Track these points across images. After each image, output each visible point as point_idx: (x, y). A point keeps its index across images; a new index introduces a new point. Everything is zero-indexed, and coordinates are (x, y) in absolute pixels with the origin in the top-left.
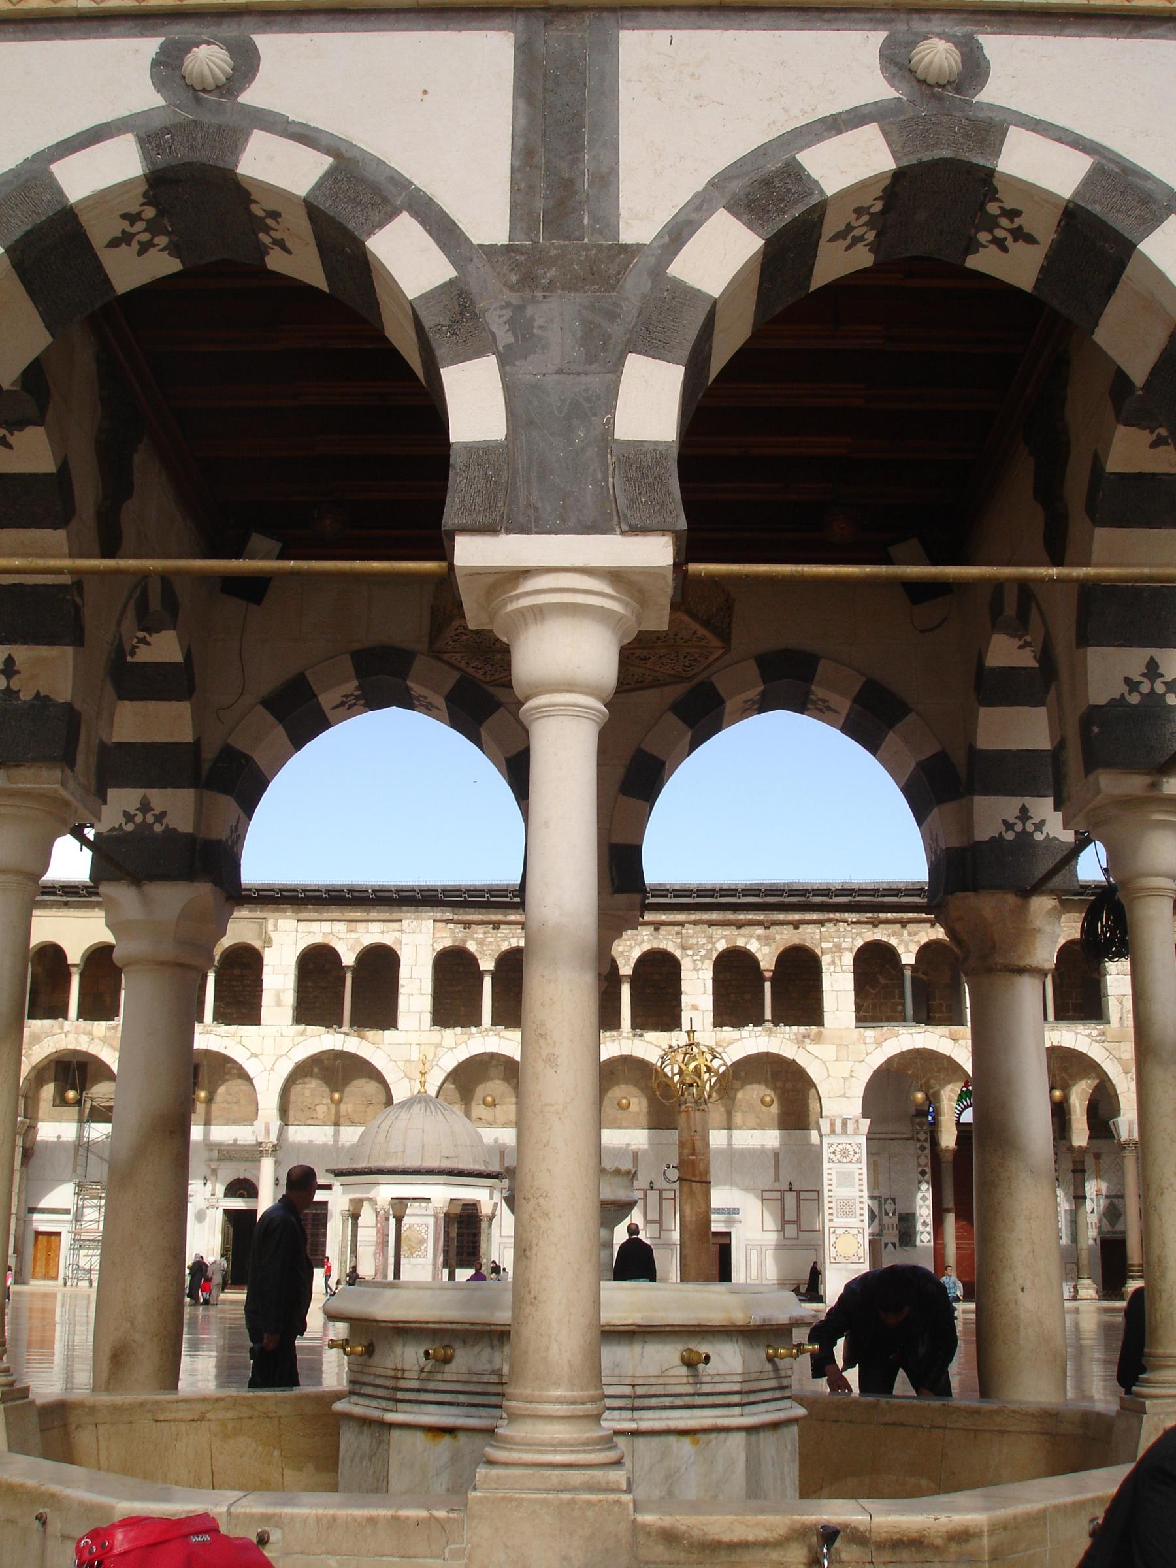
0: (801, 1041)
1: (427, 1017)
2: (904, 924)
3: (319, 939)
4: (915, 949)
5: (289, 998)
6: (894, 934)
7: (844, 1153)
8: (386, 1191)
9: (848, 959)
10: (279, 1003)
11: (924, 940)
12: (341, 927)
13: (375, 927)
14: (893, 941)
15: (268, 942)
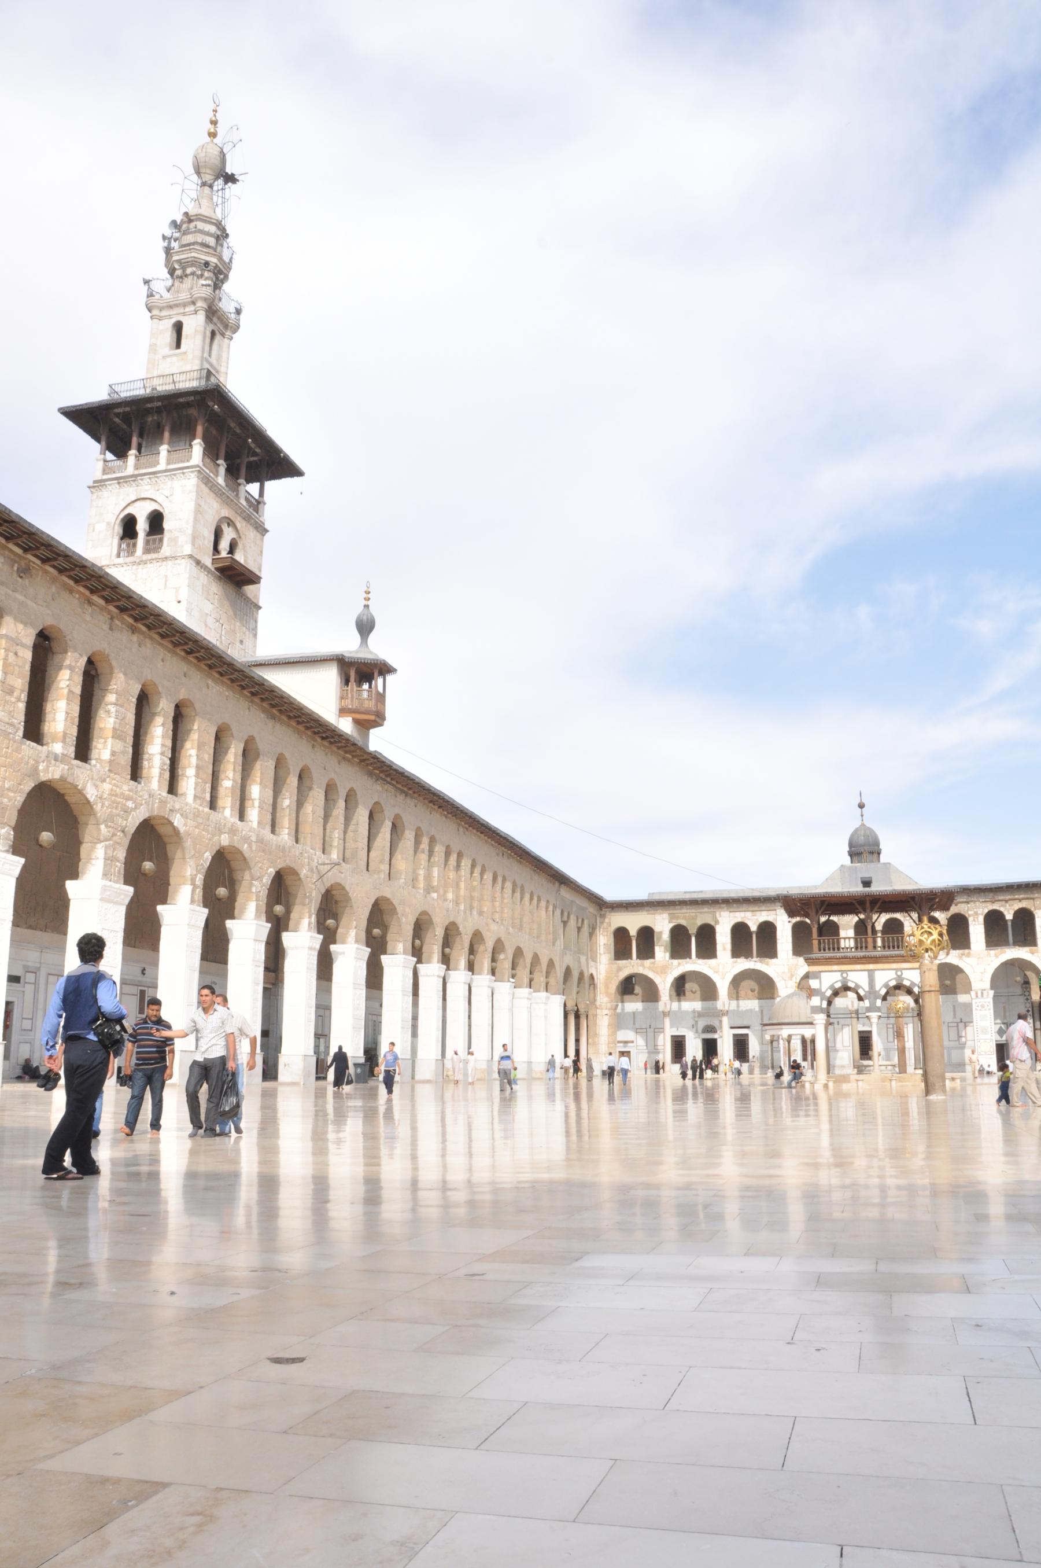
0: (960, 957)
1: (791, 952)
2: (1006, 901)
3: (739, 920)
4: (1012, 912)
5: (729, 946)
6: (1004, 906)
7: (983, 1006)
8: (785, 1032)
9: (981, 919)
10: (724, 949)
11: (1016, 908)
12: (749, 914)
13: (764, 913)
14: (1002, 909)
15: (717, 922)
